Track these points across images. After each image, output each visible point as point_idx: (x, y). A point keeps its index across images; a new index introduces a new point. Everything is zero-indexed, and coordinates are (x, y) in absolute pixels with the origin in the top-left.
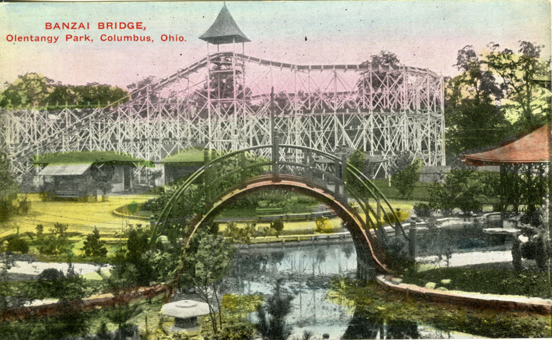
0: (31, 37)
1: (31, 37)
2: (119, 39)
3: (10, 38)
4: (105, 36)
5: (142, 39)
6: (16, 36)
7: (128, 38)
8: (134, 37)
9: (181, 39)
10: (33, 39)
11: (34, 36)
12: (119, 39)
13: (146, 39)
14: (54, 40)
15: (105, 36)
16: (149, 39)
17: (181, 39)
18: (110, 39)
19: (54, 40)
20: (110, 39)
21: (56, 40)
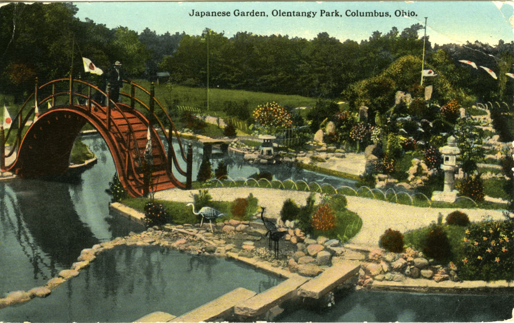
0: (294, 12)
1: (294, 12)
2: (362, 14)
3: (275, 13)
4: (350, 11)
5: (382, 15)
6: (280, 11)
7: (369, 13)
8: (375, 13)
9: (413, 14)
10: (295, 14)
11: (296, 12)
12: (362, 14)
13: (384, 14)
14: (312, 15)
15: (350, 11)
16: (387, 14)
17: (413, 14)
18: (353, 14)
19: (312, 15)
20: (353, 14)
21: (314, 15)
